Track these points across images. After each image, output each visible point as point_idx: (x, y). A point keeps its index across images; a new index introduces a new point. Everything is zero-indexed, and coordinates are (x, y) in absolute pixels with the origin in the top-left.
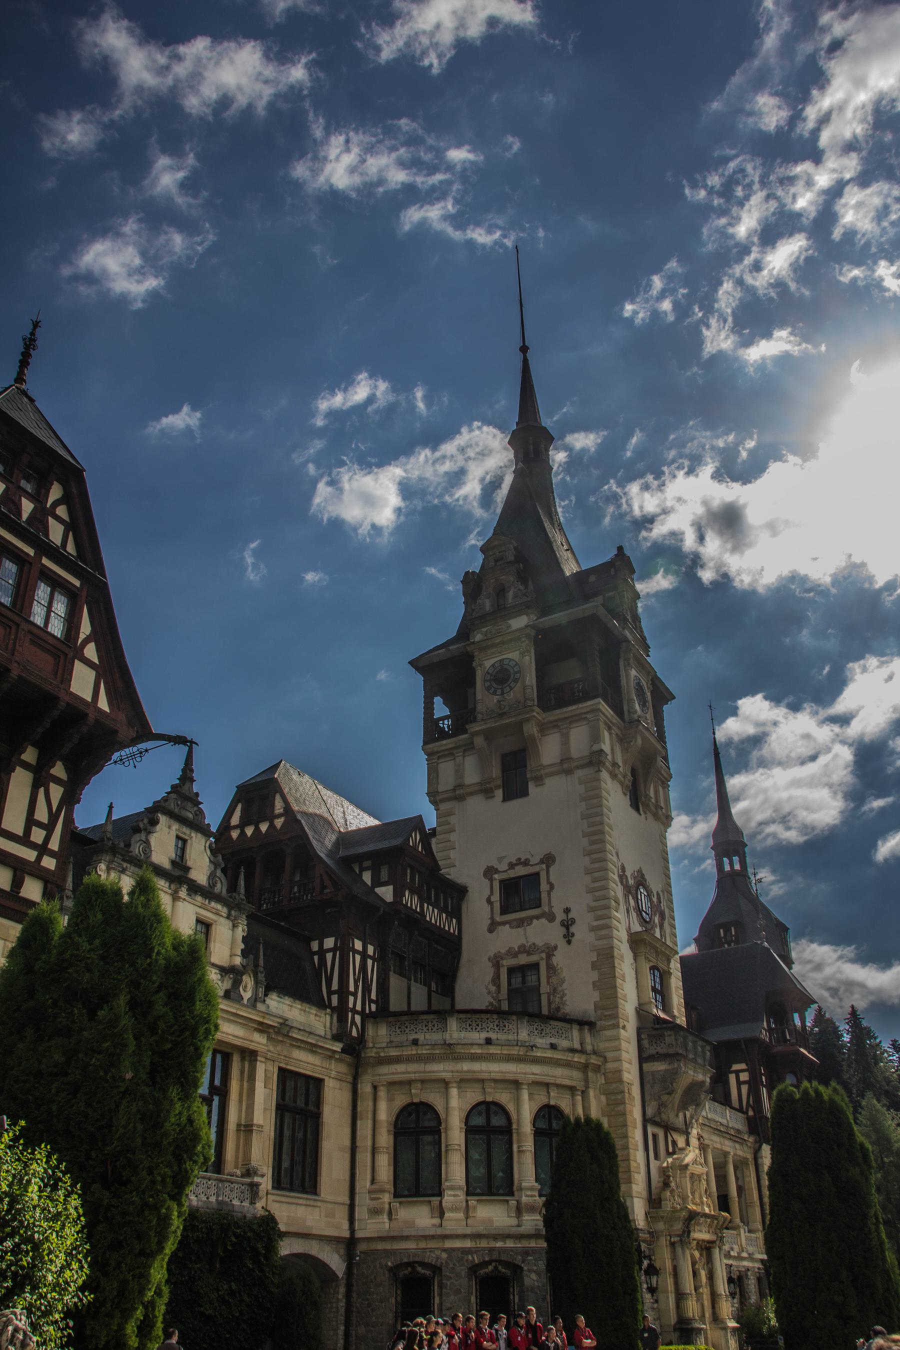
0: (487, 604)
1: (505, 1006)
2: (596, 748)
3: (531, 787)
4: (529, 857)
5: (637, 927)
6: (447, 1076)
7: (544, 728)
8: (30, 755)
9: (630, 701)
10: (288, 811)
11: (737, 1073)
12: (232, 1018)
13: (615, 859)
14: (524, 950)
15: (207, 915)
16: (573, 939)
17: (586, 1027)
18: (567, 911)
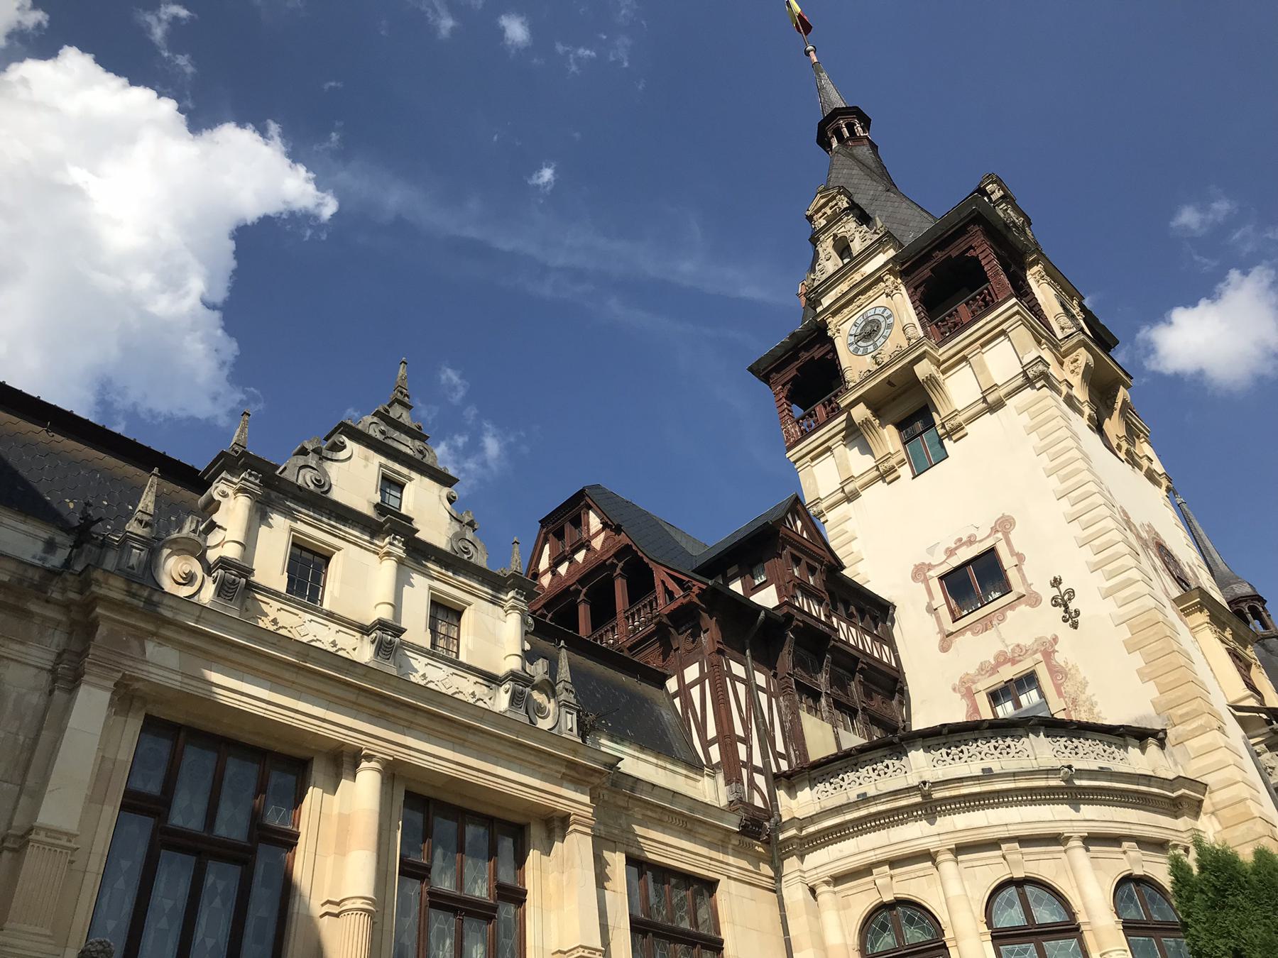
4: (973, 531)
6: (931, 844)
7: (947, 367)
12: (511, 751)
14: (1003, 659)
15: (451, 592)
17: (1151, 740)
18: (1056, 582)
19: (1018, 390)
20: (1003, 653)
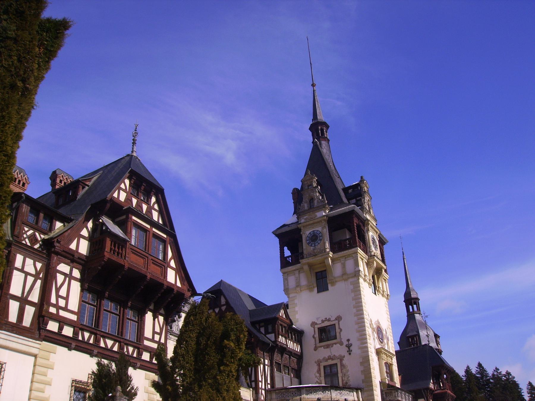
0: (306, 206)
2: (357, 269)
3: (330, 286)
4: (330, 317)
5: (378, 346)
8: (152, 307)
9: (370, 246)
10: (227, 303)
13: (367, 317)
14: (330, 358)
16: (352, 353)
18: (348, 340)
19: (352, 277)
20: (330, 356)
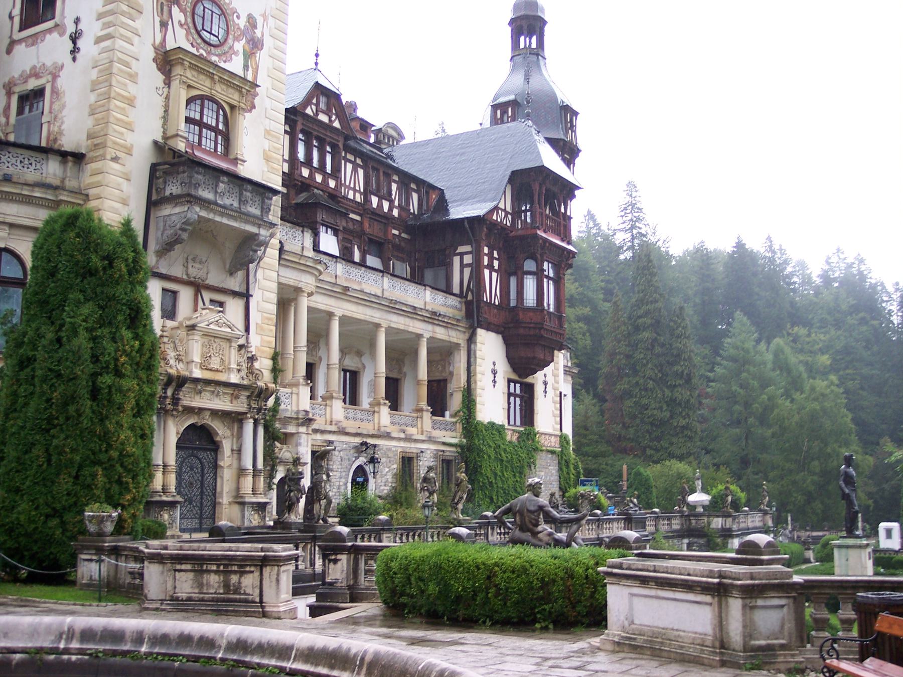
1: (11, 138)
11: (462, 255)
18: (77, 21)
